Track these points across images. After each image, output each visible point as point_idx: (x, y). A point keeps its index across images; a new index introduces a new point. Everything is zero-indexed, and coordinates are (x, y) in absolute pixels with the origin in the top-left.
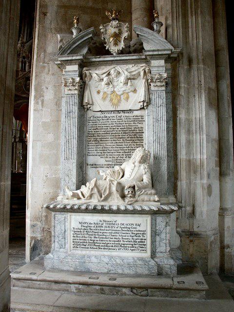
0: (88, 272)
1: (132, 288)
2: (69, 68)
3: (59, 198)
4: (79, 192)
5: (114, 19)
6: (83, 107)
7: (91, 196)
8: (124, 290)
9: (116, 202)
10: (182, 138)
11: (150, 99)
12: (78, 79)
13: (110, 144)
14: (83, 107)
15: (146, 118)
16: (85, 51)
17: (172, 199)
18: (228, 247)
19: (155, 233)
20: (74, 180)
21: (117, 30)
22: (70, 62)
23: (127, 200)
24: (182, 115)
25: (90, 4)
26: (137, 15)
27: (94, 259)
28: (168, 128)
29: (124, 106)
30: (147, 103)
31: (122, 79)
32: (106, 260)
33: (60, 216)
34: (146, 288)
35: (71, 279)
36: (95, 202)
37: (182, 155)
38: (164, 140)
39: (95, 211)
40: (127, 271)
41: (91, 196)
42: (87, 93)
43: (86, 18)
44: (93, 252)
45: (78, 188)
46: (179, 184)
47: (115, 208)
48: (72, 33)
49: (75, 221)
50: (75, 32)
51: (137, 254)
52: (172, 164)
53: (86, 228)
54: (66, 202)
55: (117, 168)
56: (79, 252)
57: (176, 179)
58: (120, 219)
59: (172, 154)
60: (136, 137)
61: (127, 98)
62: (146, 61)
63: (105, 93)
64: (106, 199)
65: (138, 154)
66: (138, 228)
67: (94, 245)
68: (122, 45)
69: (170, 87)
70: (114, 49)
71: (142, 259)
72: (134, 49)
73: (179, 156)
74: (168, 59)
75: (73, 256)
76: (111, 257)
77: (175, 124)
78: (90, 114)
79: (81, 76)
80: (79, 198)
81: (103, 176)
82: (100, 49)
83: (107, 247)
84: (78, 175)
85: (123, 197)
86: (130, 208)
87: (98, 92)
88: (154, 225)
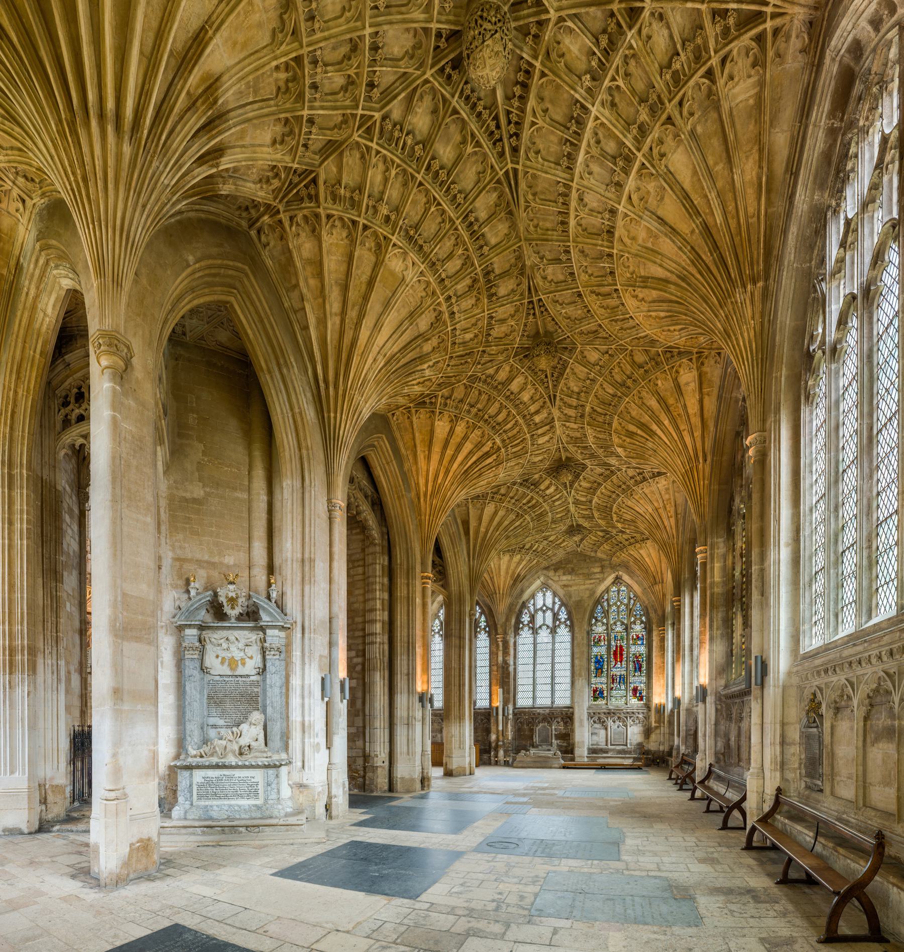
9: (232, 760)
11: (265, 666)
29: (241, 671)
35: (197, 824)
44: (215, 803)
53: (208, 781)
55: (235, 729)
56: (202, 803)
57: (288, 738)
58: (238, 773)
61: (244, 664)
76: (230, 806)
77: (288, 690)
83: (226, 797)
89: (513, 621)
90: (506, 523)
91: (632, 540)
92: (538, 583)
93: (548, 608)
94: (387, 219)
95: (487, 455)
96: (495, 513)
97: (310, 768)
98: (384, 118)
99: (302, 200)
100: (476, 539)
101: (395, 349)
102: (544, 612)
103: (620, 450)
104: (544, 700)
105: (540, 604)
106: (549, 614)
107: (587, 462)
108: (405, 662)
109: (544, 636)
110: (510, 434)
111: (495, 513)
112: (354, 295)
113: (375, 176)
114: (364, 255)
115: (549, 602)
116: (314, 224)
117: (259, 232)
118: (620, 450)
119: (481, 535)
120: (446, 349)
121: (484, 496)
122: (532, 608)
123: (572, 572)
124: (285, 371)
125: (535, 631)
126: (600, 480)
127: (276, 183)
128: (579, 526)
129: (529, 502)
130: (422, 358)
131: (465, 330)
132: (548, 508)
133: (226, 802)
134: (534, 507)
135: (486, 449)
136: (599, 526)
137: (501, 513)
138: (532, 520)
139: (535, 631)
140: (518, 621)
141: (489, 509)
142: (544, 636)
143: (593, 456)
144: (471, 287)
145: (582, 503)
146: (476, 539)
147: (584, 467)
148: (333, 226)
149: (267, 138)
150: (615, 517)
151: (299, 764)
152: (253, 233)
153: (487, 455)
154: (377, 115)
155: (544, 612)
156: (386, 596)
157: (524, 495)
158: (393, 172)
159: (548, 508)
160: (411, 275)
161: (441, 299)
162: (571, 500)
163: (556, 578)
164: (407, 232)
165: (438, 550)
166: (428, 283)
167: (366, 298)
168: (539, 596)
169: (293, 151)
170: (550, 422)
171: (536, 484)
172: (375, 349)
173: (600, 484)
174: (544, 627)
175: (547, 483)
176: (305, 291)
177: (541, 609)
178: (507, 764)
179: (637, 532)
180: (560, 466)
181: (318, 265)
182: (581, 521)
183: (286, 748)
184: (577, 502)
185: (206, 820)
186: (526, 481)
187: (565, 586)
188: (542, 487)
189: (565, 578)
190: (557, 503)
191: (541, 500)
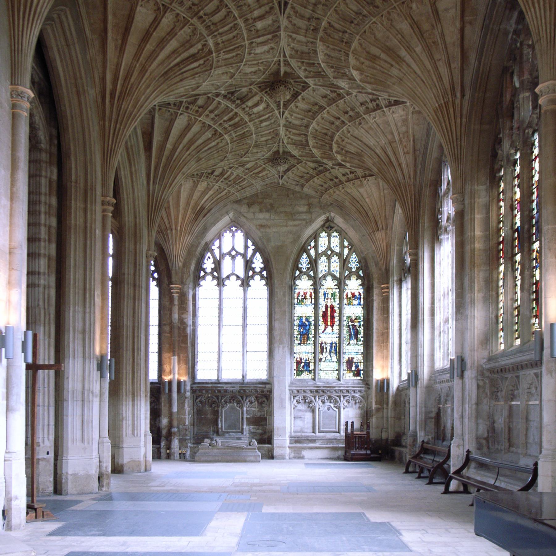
89: (193, 267)
92: (226, 219)
95: (194, 58)
96: (188, 128)
100: (159, 157)
106: (240, 261)
107: (310, 81)
110: (224, 38)
111: (188, 128)
119: (167, 153)
121: (178, 105)
123: (271, 208)
126: (323, 103)
128: (287, 153)
129: (231, 119)
132: (253, 129)
134: (236, 126)
135: (193, 50)
136: (313, 155)
137: (195, 128)
138: (232, 141)
139: (221, 282)
140: (199, 267)
141: (181, 122)
143: (319, 74)
145: (295, 127)
146: (159, 157)
147: (306, 86)
150: (335, 148)
153: (194, 58)
155: (233, 258)
157: (227, 110)
162: (282, 122)
163: (250, 216)
168: (227, 235)
170: (274, 32)
171: (243, 99)
173: (322, 108)
174: (233, 278)
175: (256, 99)
182: (291, 149)
184: (288, 126)
186: (232, 93)
187: (261, 226)
188: (250, 103)
189: (261, 216)
190: (264, 124)
191: (247, 119)
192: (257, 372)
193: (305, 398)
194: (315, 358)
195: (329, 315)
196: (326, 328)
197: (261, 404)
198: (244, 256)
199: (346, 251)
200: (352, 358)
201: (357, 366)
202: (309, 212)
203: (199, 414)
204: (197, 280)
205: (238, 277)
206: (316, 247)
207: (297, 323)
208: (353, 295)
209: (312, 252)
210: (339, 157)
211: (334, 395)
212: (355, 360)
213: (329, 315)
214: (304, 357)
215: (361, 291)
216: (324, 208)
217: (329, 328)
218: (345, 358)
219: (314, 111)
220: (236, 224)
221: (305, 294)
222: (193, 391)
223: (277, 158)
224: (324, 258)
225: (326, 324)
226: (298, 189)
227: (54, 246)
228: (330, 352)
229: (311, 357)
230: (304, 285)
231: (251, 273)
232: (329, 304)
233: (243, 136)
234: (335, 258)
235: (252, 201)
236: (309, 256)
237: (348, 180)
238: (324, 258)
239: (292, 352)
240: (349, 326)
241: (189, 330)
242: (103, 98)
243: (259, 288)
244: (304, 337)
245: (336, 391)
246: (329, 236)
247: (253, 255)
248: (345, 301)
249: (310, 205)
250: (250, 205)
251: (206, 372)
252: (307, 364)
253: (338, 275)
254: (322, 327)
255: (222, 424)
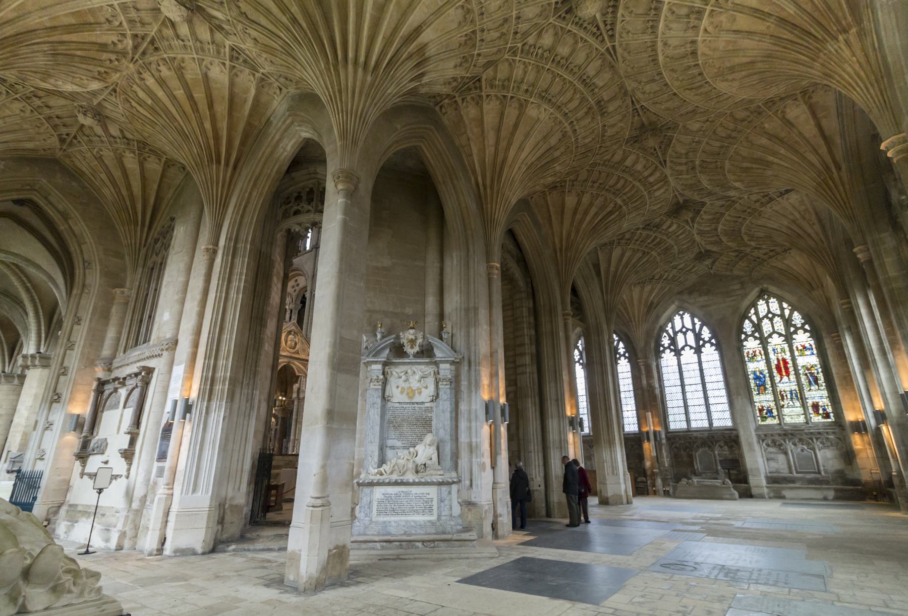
0: (389, 534)
1: (423, 541)
2: (374, 367)
3: (362, 476)
4: (382, 469)
5: (411, 328)
6: (385, 398)
7: (392, 473)
8: (417, 544)
9: (410, 477)
10: (463, 425)
11: (438, 394)
12: (381, 377)
13: (405, 429)
14: (385, 398)
15: (435, 409)
16: (387, 351)
17: (454, 474)
18: (501, 516)
19: (441, 500)
20: (376, 459)
21: (413, 337)
22: (376, 362)
23: (420, 474)
24: (463, 407)
25: (391, 309)
26: (431, 321)
27: (393, 524)
28: (451, 417)
29: (417, 399)
30: (436, 397)
31: (417, 377)
32: (403, 524)
33: (367, 490)
34: (433, 541)
35: (377, 538)
36: (394, 477)
37: (463, 438)
38: (448, 428)
39: (396, 483)
40: (419, 531)
41: (392, 473)
42: (388, 388)
43: (387, 321)
44: (393, 518)
45: (380, 466)
46: (459, 462)
47: (411, 481)
48: (376, 336)
49: (379, 493)
50: (379, 336)
51: (427, 518)
52: (454, 446)
53: (388, 498)
54: (372, 477)
55: (412, 449)
56: (382, 519)
57: (457, 457)
58: (415, 490)
59: (454, 438)
60: (426, 424)
61: (420, 393)
62: (436, 364)
63: (403, 388)
64: (404, 474)
65: (429, 438)
66: (428, 496)
67: (394, 512)
68: (417, 349)
69: (453, 385)
70: (410, 351)
71: (430, 521)
72: (426, 352)
73: (460, 440)
74: (453, 363)
75: (377, 522)
76: (407, 521)
77: (457, 414)
78: (389, 405)
79: (383, 374)
80: (381, 474)
81: (399, 458)
82: (398, 351)
83: (404, 513)
84: (379, 455)
85: (417, 472)
86: (423, 480)
87: (398, 387)
88: (439, 494)
89: (653, 345)
90: (634, 261)
91: (771, 254)
92: (673, 307)
93: (688, 330)
94: (527, 91)
95: (611, 213)
96: (623, 255)
97: (477, 486)
98: (523, 45)
99: (470, 90)
100: (607, 278)
101: (534, 159)
102: (685, 334)
103: (737, 184)
104: (699, 421)
105: (678, 327)
106: (690, 336)
107: (706, 200)
108: (553, 390)
109: (688, 356)
110: (628, 195)
111: (623, 255)
112: (504, 133)
113: (518, 72)
114: (511, 113)
115: (689, 325)
116: (478, 101)
117: (441, 107)
118: (737, 184)
119: (611, 274)
120: (571, 152)
121: (611, 243)
122: (671, 332)
123: (708, 293)
124: (455, 182)
125: (678, 353)
126: (722, 210)
127: (455, 84)
128: (707, 251)
129: (653, 241)
130: (554, 160)
131: (584, 138)
132: (672, 243)
133: (404, 518)
134: (659, 244)
135: (609, 209)
136: (730, 248)
137: (628, 254)
138: (659, 254)
139: (678, 353)
140: (658, 343)
141: (617, 253)
142: (688, 356)
143: (710, 194)
144: (587, 113)
145: (708, 232)
146: (607, 278)
147: (703, 204)
148: (491, 100)
149: (452, 64)
150: (746, 238)
151: (468, 483)
152: (437, 108)
153: (611, 213)
154: (520, 45)
155: (685, 334)
156: (533, 332)
157: (648, 236)
158: (530, 68)
159: (672, 243)
160: (543, 116)
161: (566, 124)
162: (695, 232)
163: (692, 301)
164: (540, 94)
165: (574, 291)
166: (556, 118)
167: (513, 134)
168: (677, 319)
169: (467, 69)
170: (664, 179)
171: (658, 226)
172: (520, 161)
173: (722, 214)
174: (687, 348)
175: (668, 223)
176: (470, 135)
177: (681, 331)
178: (667, 494)
179: (776, 246)
180: (678, 209)
181: (480, 122)
182: (709, 247)
183: (456, 467)
184: (701, 233)
185: (383, 535)
186: (648, 225)
187: (702, 306)
188: (664, 227)
189: (701, 299)
190: (681, 237)
191: (665, 237)
192: (722, 419)
193: (774, 442)
194: (776, 404)
195: (782, 368)
196: (781, 378)
197: (731, 447)
198: (693, 330)
199: (787, 312)
200: (818, 403)
201: (824, 410)
202: (743, 288)
203: (676, 458)
204: (658, 354)
205: (691, 348)
206: (757, 313)
207: (751, 376)
208: (804, 347)
209: (754, 318)
210: (753, 244)
211: (804, 437)
212: (820, 404)
213: (782, 368)
214: (765, 404)
215: (812, 342)
216: (756, 282)
217: (785, 379)
218: (810, 402)
219: (716, 220)
220: (682, 308)
221: (754, 352)
222: (668, 439)
223: (701, 256)
224: (766, 321)
225: (781, 375)
226: (728, 273)
227: (534, 347)
228: (792, 399)
229: (772, 404)
230: (752, 345)
231: (701, 342)
232: (780, 358)
233: (667, 249)
234: (777, 319)
235: (691, 291)
236: (752, 321)
237: (771, 257)
238: (766, 321)
239: (752, 402)
240: (806, 374)
241: (657, 391)
242: (556, 253)
243: (710, 354)
244: (762, 387)
245: (806, 434)
246: (767, 303)
247: (701, 329)
248: (796, 353)
249: (742, 283)
250: (690, 293)
251: (677, 423)
252: (770, 411)
253: (784, 333)
254: (777, 378)
255: (698, 466)
